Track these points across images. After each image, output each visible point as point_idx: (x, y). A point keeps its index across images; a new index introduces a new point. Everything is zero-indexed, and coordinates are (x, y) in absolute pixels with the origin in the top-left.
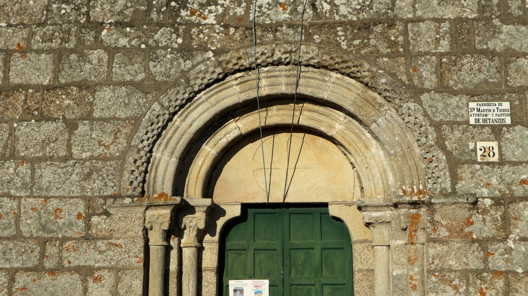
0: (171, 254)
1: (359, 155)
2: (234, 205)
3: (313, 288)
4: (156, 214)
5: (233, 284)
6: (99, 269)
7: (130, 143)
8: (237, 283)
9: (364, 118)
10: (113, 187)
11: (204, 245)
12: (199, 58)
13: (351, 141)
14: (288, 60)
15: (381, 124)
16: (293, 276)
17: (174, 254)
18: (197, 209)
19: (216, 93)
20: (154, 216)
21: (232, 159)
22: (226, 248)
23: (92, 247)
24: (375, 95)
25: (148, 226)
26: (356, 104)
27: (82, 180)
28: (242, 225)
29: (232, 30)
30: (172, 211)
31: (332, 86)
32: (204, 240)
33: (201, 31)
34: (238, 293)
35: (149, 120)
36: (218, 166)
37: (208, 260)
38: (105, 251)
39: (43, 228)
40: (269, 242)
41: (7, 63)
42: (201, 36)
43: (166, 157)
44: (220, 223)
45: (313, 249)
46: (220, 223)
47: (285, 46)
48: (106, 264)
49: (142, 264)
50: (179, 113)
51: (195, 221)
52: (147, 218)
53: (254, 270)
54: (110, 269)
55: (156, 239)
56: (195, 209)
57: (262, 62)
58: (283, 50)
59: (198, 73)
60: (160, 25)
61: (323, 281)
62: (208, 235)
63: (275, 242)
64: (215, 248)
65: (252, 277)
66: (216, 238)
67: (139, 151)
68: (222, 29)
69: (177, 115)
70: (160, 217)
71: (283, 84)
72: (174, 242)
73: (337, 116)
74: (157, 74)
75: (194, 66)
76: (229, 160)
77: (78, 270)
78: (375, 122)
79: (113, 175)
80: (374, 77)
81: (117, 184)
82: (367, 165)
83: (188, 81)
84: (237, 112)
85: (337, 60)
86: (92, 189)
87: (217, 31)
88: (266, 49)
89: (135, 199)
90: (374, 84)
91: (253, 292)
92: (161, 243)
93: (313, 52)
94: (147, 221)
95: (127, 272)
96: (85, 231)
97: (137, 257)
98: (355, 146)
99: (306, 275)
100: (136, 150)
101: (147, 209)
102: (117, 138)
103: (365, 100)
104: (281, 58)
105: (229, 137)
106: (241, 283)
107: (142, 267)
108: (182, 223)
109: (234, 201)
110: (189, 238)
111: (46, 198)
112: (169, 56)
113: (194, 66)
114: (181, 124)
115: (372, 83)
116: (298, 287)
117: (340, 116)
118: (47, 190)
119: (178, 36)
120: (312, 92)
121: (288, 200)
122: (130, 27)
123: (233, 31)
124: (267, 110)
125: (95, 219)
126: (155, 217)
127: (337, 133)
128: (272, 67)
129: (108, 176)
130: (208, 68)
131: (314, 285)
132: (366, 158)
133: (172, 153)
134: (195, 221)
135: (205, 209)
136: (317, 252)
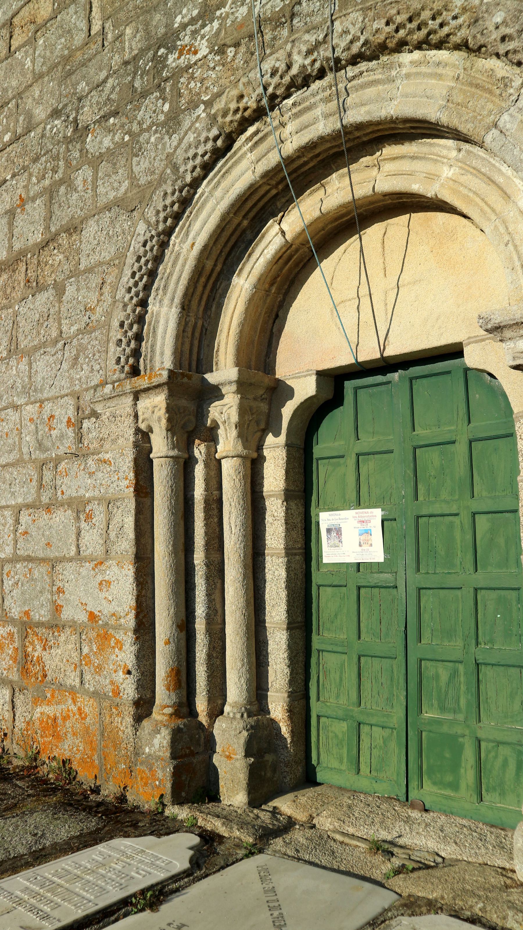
0: (196, 470)
1: (489, 220)
2: (305, 376)
3: (456, 520)
4: (149, 405)
5: (325, 519)
6: (89, 501)
7: (115, 297)
8: (331, 518)
9: (470, 126)
10: (99, 371)
11: (266, 453)
12: (187, 124)
13: (471, 194)
14: (317, 65)
15: (508, 126)
16: (421, 498)
17: (199, 471)
18: (224, 391)
19: (223, 176)
20: (148, 409)
21: (299, 297)
22: (315, 456)
23: (82, 468)
24: (493, 63)
25: (143, 426)
26: (453, 103)
27: (70, 368)
28: (337, 413)
29: (231, 52)
30: (171, 395)
31: (411, 85)
32: (266, 444)
33: (192, 78)
34: (334, 534)
35: (135, 252)
36: (280, 314)
37: (271, 479)
38: (94, 473)
39: (40, 445)
40: (381, 438)
41: (11, 224)
42: (192, 85)
43: (165, 309)
44: (287, 411)
45: (454, 442)
46: (287, 411)
47: (307, 37)
48: (96, 493)
49: (132, 489)
50: (177, 229)
51: (225, 411)
52: (140, 414)
53: (359, 492)
54: (100, 500)
55: (160, 445)
56: (220, 390)
57: (275, 88)
58: (304, 49)
59: (186, 151)
60: (144, 95)
61: (475, 506)
62: (270, 434)
63: (391, 437)
64: (280, 457)
65: (359, 504)
66: (282, 439)
67: (125, 306)
68: (217, 58)
69: (175, 234)
70: (156, 410)
71: (320, 117)
72: (200, 451)
73: (445, 152)
74: (141, 174)
75: (181, 140)
76: (295, 298)
77: (69, 503)
78: (496, 126)
79: (99, 352)
80: (476, 21)
81: (103, 366)
82: (507, 238)
83: (175, 168)
84: (279, 205)
85: (399, 19)
86: (80, 379)
87: (212, 65)
88: (277, 60)
89: (116, 384)
90: (479, 36)
91: (357, 532)
92: (172, 453)
93: (354, 25)
94: (140, 421)
95: (118, 504)
96: (75, 444)
97: (126, 479)
98: (482, 204)
99: (444, 495)
100: (121, 305)
101: (136, 398)
102: (101, 295)
103: (471, 84)
104: (304, 66)
105: (268, 253)
106: (337, 517)
107: (132, 495)
108: (208, 417)
109: (305, 369)
110: (228, 442)
111: (42, 402)
112: (153, 139)
113: (181, 140)
114: (182, 248)
115: (474, 37)
116: (432, 520)
117: (445, 147)
118: (42, 391)
119: (164, 100)
120: (368, 112)
121: (389, 352)
122: (113, 116)
123: (233, 53)
124: (323, 186)
125: (86, 424)
126: (150, 411)
127: (442, 185)
128: (299, 92)
129: (94, 355)
130: (199, 135)
131: (456, 515)
132: (504, 222)
133: (173, 300)
134: (225, 411)
135: (234, 387)
136: (461, 449)
